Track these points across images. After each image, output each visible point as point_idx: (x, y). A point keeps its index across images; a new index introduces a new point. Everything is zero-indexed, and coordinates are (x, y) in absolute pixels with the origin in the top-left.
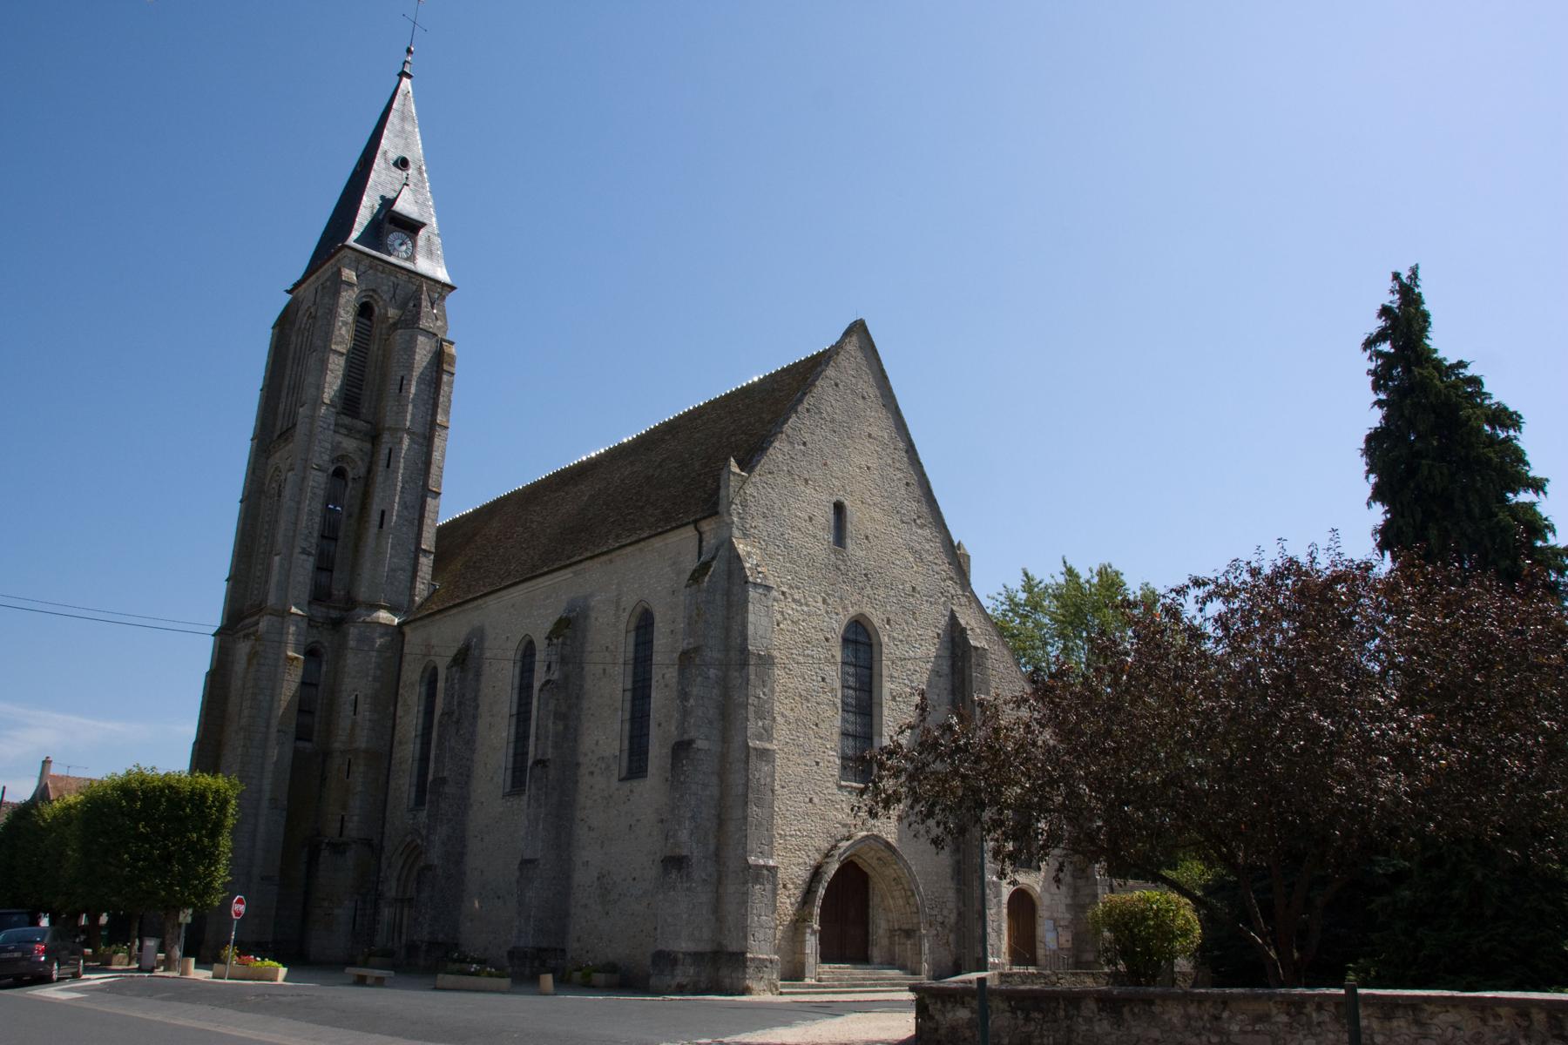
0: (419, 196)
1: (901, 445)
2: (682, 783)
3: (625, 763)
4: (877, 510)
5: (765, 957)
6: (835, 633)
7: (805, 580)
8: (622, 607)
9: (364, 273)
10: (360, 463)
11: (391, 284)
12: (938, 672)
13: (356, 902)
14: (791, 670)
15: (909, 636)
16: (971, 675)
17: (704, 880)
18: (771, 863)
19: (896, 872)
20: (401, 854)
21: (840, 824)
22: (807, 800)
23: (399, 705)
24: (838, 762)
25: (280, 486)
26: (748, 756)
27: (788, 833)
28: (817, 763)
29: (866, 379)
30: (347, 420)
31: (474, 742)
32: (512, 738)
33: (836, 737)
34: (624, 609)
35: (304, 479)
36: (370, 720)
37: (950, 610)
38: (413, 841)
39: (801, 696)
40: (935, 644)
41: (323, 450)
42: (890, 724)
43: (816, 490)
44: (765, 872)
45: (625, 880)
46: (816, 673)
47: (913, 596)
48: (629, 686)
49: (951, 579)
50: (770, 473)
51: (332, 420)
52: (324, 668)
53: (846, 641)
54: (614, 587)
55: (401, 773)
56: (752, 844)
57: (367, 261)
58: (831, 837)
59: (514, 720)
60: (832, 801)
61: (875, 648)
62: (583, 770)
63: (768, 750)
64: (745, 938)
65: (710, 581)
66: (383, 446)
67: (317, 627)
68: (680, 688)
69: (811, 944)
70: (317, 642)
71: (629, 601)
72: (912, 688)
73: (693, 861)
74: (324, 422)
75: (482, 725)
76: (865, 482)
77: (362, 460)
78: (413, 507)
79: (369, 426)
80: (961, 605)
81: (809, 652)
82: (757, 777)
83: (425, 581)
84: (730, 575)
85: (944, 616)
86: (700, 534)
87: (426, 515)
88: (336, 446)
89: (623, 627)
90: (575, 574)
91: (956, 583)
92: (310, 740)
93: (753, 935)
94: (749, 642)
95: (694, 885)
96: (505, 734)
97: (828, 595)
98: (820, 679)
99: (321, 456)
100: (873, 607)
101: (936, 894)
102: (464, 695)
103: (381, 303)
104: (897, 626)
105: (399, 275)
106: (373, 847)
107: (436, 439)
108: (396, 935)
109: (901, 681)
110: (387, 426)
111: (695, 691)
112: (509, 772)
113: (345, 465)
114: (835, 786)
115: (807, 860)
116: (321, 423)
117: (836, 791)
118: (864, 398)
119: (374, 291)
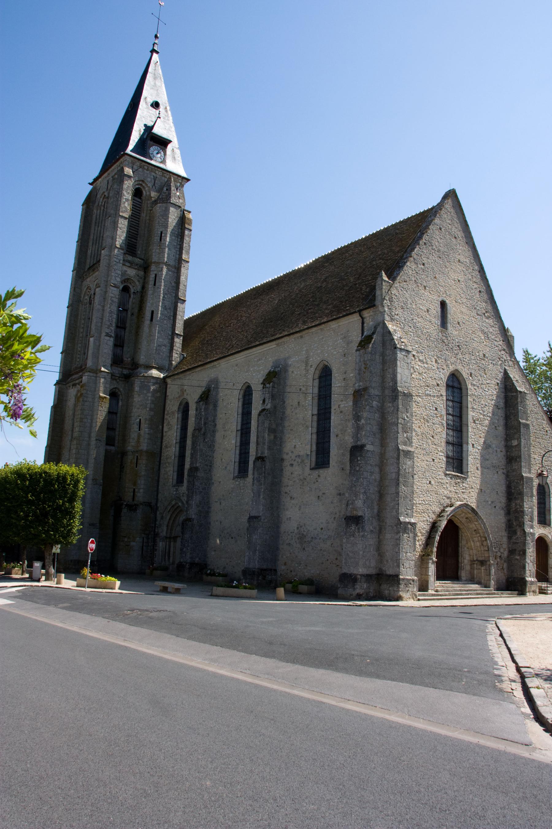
0: (166, 125)
1: (476, 268)
2: (358, 471)
3: (314, 459)
4: (464, 307)
5: (410, 578)
6: (442, 381)
7: (425, 348)
8: (310, 364)
9: (137, 170)
10: (137, 283)
11: (153, 177)
12: (497, 406)
13: (143, 538)
14: (418, 403)
16: (518, 408)
17: (372, 531)
18: (413, 521)
19: (476, 527)
20: (169, 511)
22: (428, 482)
23: (165, 425)
24: (445, 459)
25: (90, 297)
26: (399, 455)
27: (418, 503)
28: (433, 460)
29: (456, 226)
30: (130, 258)
31: (214, 446)
32: (238, 444)
33: (443, 444)
34: (311, 366)
35: (106, 292)
36: (148, 434)
37: (503, 369)
38: (176, 504)
39: (424, 419)
40: (496, 389)
41: (117, 275)
42: (472, 437)
43: (430, 293)
44: (409, 526)
45: (316, 529)
46: (432, 405)
47: (484, 360)
48: (315, 412)
49: (504, 350)
50: (405, 281)
51: (121, 257)
52: (120, 403)
53: (448, 386)
54: (304, 352)
55: (167, 465)
56: (402, 509)
57: (138, 163)
58: (441, 505)
59: (239, 433)
60: (442, 483)
61: (464, 391)
62: (286, 463)
63: (410, 451)
64: (398, 566)
65: (373, 347)
66: (152, 273)
67: (116, 380)
68: (354, 413)
69: (432, 569)
70: (115, 388)
71: (315, 360)
72: (484, 415)
73: (365, 519)
74: (117, 259)
75: (218, 436)
76: (457, 289)
77: (139, 281)
78: (170, 309)
79: (142, 261)
80: (510, 366)
81: (428, 392)
82: (404, 468)
83: (178, 353)
84: (384, 343)
85: (501, 372)
86: (363, 318)
87: (178, 314)
88: (124, 273)
89: (310, 377)
90: (278, 345)
91: (506, 352)
92: (113, 445)
93: (403, 565)
94: (398, 385)
95: (366, 534)
96: (234, 442)
97: (438, 357)
98: (434, 409)
99: (116, 279)
100: (463, 366)
101: (497, 540)
102: (207, 419)
103: (147, 189)
104: (476, 378)
105: (157, 172)
106: (152, 507)
107: (182, 269)
108: (167, 557)
109: (478, 411)
110: (153, 261)
111: (365, 415)
112: (237, 464)
113: (129, 285)
115: (428, 519)
116: (115, 259)
117: (443, 477)
119: (143, 181)
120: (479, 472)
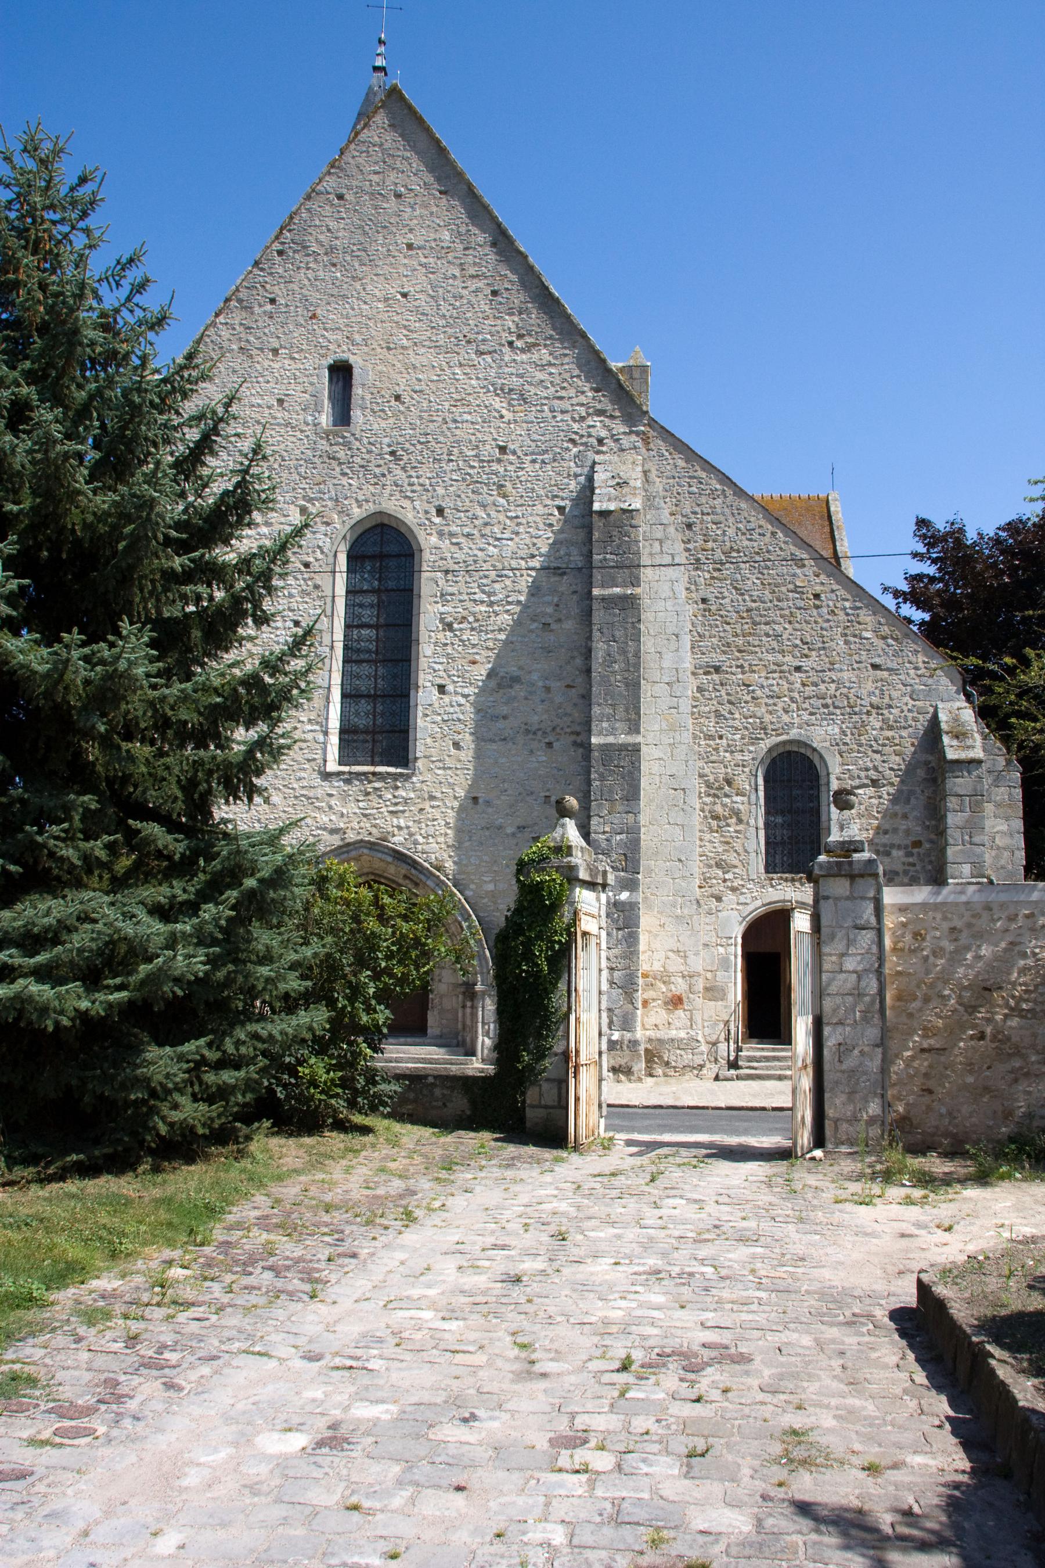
1: (481, 238)
4: (423, 350)
6: (322, 552)
15: (486, 524)
21: (325, 829)
29: (405, 166)
40: (551, 525)
42: (437, 667)
43: (294, 359)
47: (499, 461)
49: (600, 413)
60: (309, 798)
72: (491, 604)
80: (623, 450)
85: (576, 476)
91: (612, 417)
97: (311, 500)
98: (291, 625)
100: (407, 497)
114: (315, 775)
118: (398, 196)
120: (467, 755)
